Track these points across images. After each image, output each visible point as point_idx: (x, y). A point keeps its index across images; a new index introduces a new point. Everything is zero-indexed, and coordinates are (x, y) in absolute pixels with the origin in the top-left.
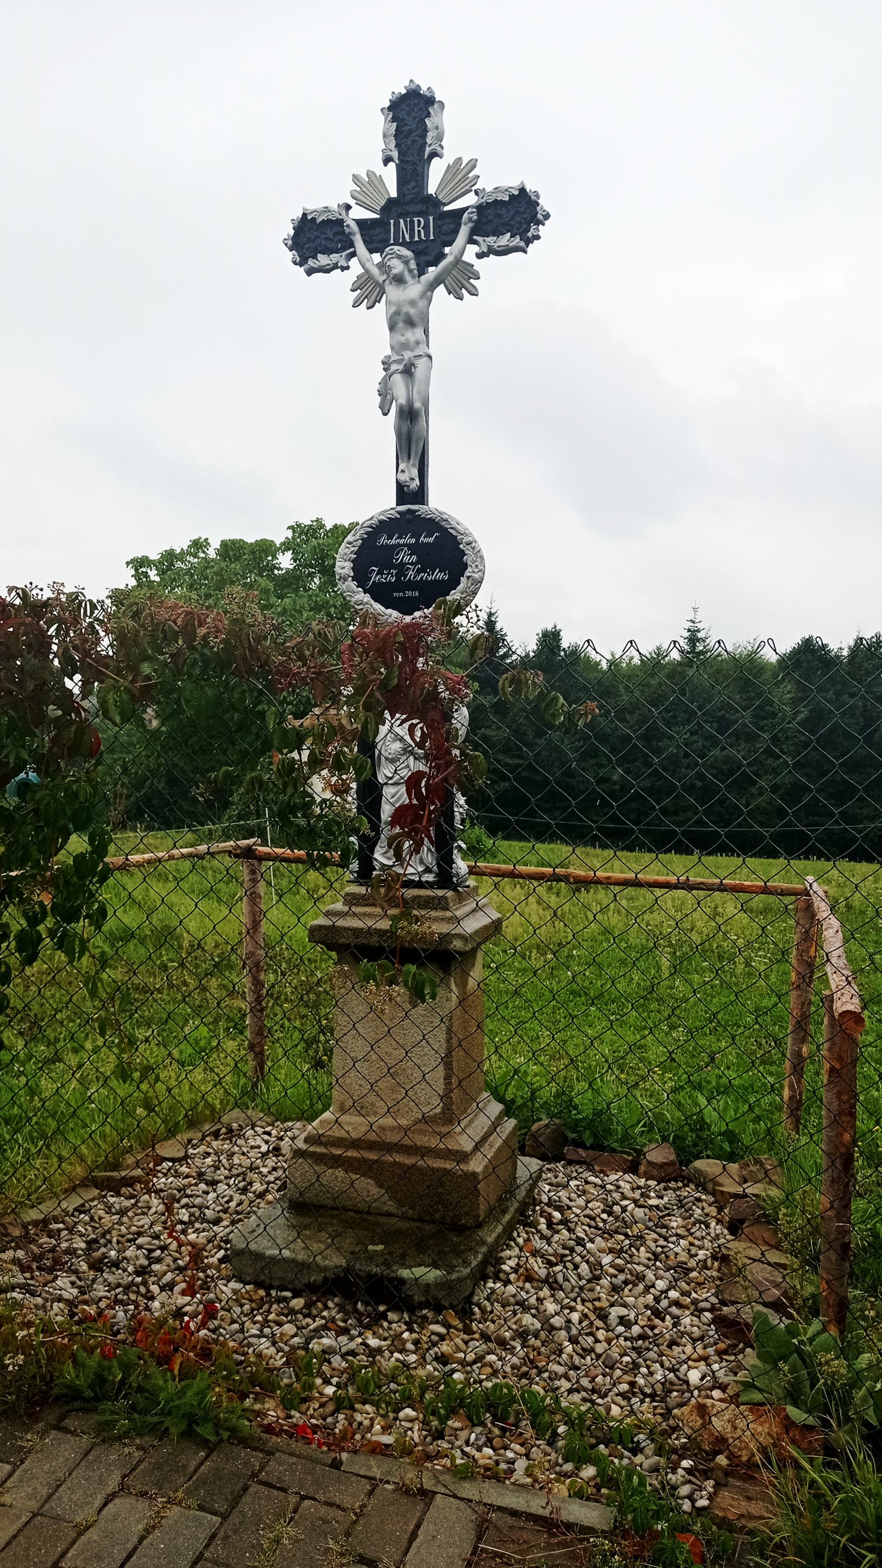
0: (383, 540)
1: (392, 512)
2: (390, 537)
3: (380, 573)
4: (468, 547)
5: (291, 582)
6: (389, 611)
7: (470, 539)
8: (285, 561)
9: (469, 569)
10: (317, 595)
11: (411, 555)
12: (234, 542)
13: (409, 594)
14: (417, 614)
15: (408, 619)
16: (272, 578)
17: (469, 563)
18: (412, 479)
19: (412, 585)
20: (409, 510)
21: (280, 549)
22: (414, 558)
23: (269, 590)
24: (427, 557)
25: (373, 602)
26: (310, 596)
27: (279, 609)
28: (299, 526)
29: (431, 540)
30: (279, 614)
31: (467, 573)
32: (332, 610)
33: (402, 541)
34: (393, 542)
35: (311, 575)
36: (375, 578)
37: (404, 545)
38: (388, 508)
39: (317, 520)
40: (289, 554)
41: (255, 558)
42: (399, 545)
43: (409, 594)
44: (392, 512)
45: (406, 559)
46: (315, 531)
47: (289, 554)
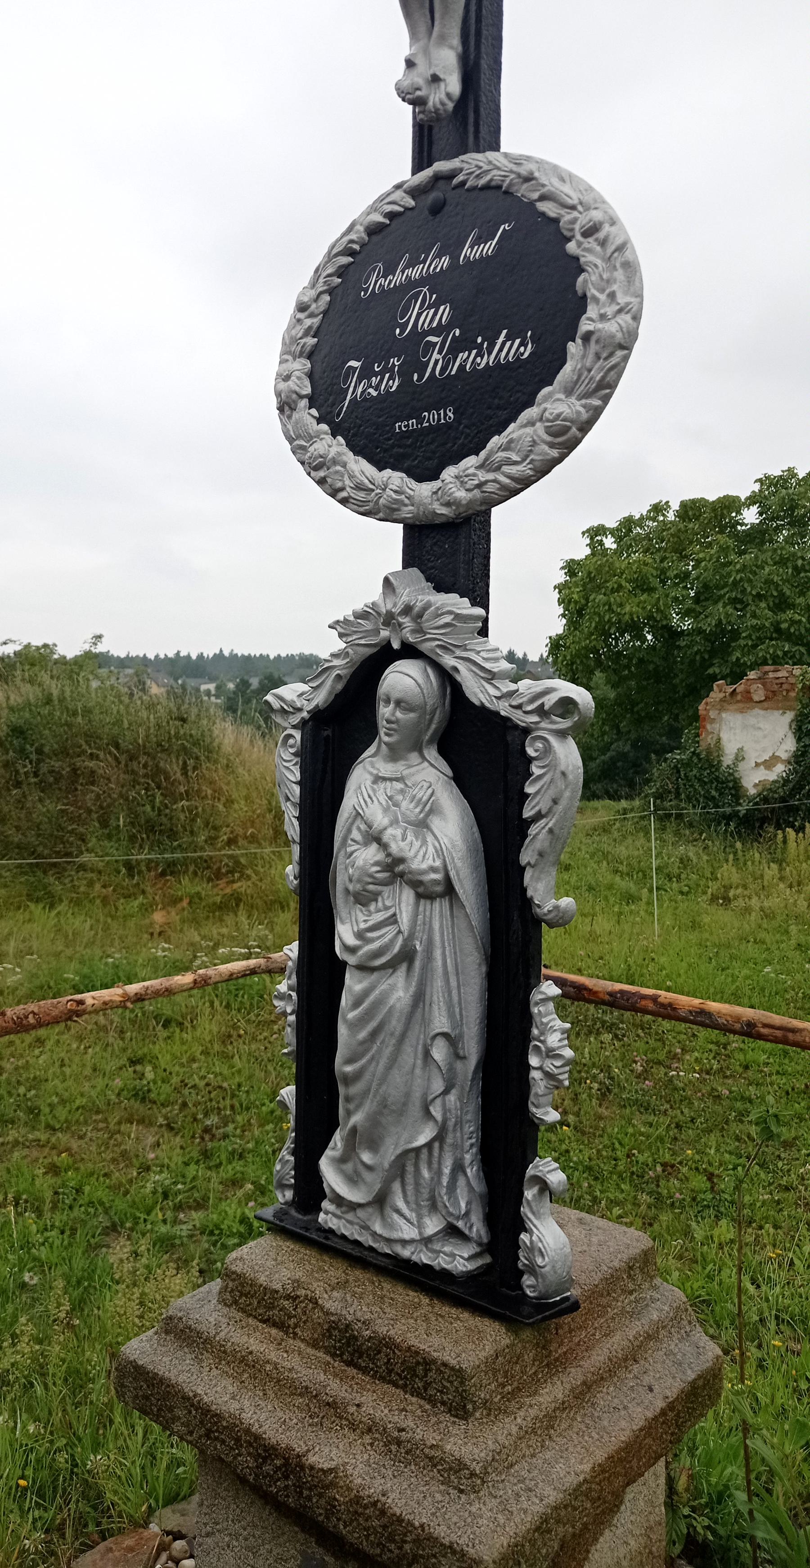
0: (376, 282)
1: (398, 195)
2: (390, 270)
3: (366, 373)
4: (590, 243)
5: (757, 536)
6: (388, 472)
7: (596, 215)
8: (751, 516)
9: (592, 311)
10: (782, 549)
11: (436, 305)
12: (693, 501)
13: (431, 418)
14: (449, 473)
15: (424, 490)
16: (735, 535)
17: (592, 291)
18: (435, 79)
19: (443, 390)
20: (438, 178)
21: (744, 504)
22: (445, 312)
23: (728, 547)
24: (478, 305)
25: (349, 456)
26: (775, 550)
27: (738, 566)
28: (767, 477)
29: (489, 248)
30: (738, 571)
31: (585, 326)
32: (800, 562)
33: (415, 273)
34: (398, 278)
35: (778, 529)
36: (355, 389)
37: (422, 281)
38: (388, 187)
39: (789, 470)
40: (754, 509)
41: (716, 517)
42: (411, 284)
43: (431, 418)
44: (399, 194)
45: (426, 320)
46: (786, 481)
47: (754, 509)
